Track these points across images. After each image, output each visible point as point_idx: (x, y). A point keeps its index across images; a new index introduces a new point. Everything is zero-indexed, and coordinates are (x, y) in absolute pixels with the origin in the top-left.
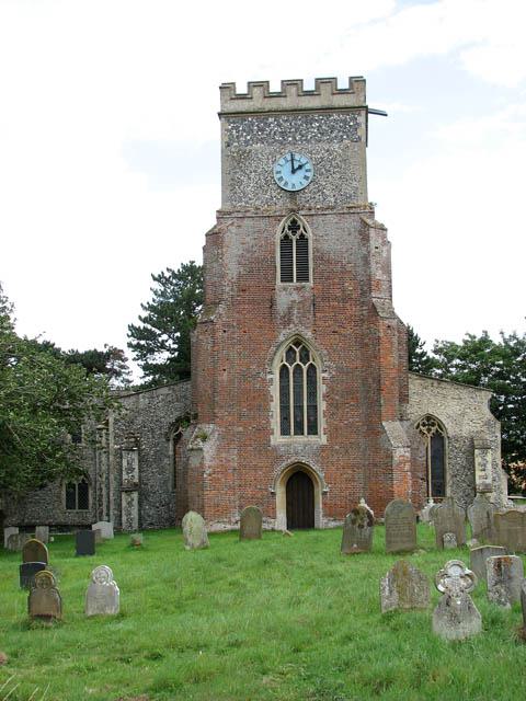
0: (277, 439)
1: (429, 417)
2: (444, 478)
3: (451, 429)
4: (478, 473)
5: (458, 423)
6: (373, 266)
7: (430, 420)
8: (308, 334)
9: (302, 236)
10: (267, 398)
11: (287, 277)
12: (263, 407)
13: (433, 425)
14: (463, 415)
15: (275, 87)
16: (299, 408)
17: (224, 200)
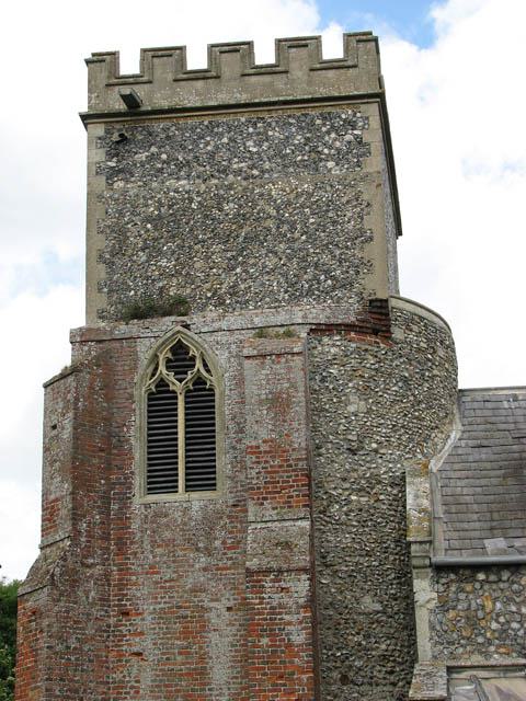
9: (199, 381)
15: (197, 60)
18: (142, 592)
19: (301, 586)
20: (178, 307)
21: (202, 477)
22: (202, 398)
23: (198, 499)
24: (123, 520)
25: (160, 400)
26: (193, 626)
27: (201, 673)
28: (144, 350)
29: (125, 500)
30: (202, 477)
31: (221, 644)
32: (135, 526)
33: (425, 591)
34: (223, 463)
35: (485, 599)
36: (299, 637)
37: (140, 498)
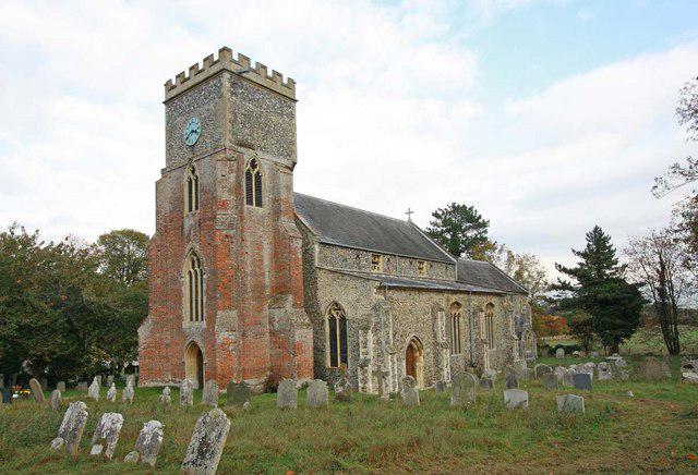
0: (186, 323)
1: (337, 304)
2: (346, 352)
3: (349, 314)
4: (362, 350)
5: (355, 308)
6: (219, 189)
7: (336, 305)
8: (197, 248)
10: (179, 294)
11: (190, 210)
12: (179, 302)
13: (339, 309)
14: (358, 301)
16: (197, 300)
17: (168, 160)
18: (247, 234)
19: (300, 242)
20: (250, 147)
21: (259, 204)
22: (258, 177)
23: (260, 210)
24: (241, 212)
25: (248, 173)
26: (260, 248)
27: (261, 261)
28: (245, 157)
29: (242, 204)
30: (259, 204)
31: (267, 252)
32: (245, 213)
33: (317, 248)
34: (266, 199)
35: (327, 251)
36: (300, 257)
37: (246, 206)
